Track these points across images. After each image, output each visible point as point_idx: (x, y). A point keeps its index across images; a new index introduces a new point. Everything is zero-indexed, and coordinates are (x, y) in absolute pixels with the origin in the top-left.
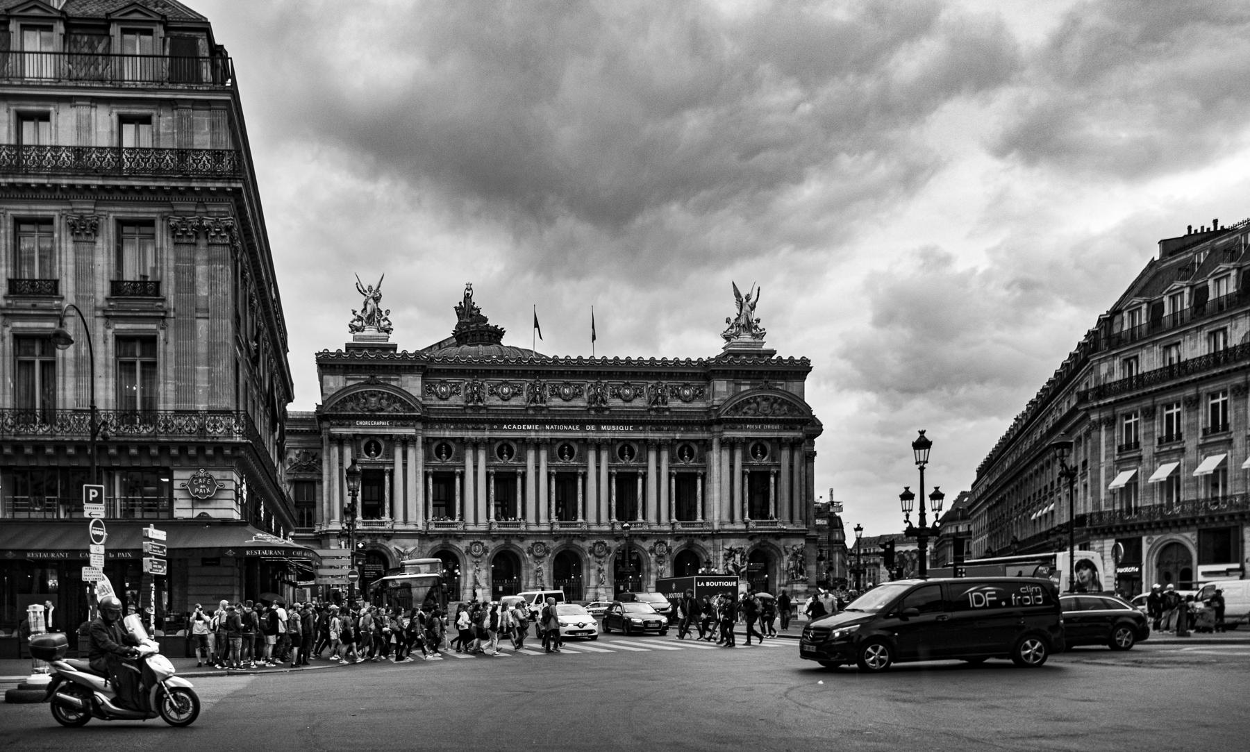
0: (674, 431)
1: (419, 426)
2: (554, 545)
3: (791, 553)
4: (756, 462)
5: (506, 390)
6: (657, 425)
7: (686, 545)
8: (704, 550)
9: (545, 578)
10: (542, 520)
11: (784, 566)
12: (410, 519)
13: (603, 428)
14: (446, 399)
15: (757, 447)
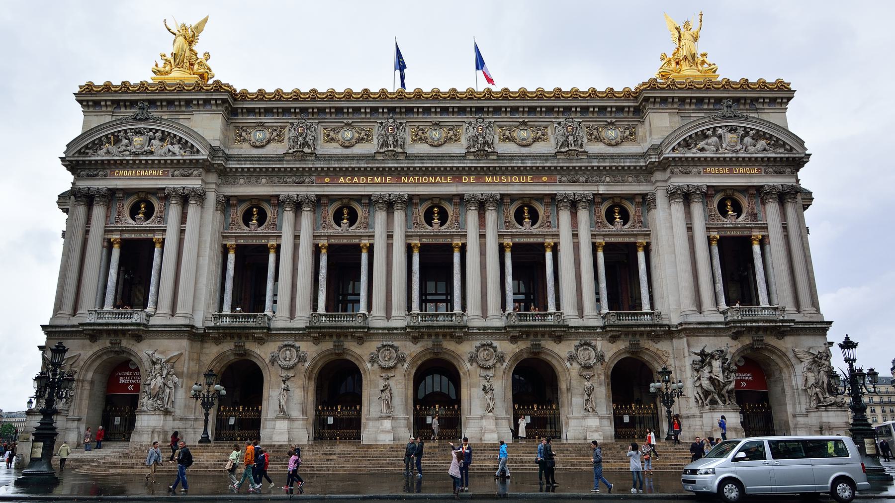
0: (596, 183)
1: (213, 178)
2: (411, 349)
3: (807, 360)
4: (728, 222)
5: (348, 135)
6: (572, 174)
7: (626, 351)
8: (657, 356)
9: (398, 402)
10: (394, 313)
11: (798, 381)
12: (179, 310)
13: (488, 179)
14: (262, 147)
15: (728, 200)
